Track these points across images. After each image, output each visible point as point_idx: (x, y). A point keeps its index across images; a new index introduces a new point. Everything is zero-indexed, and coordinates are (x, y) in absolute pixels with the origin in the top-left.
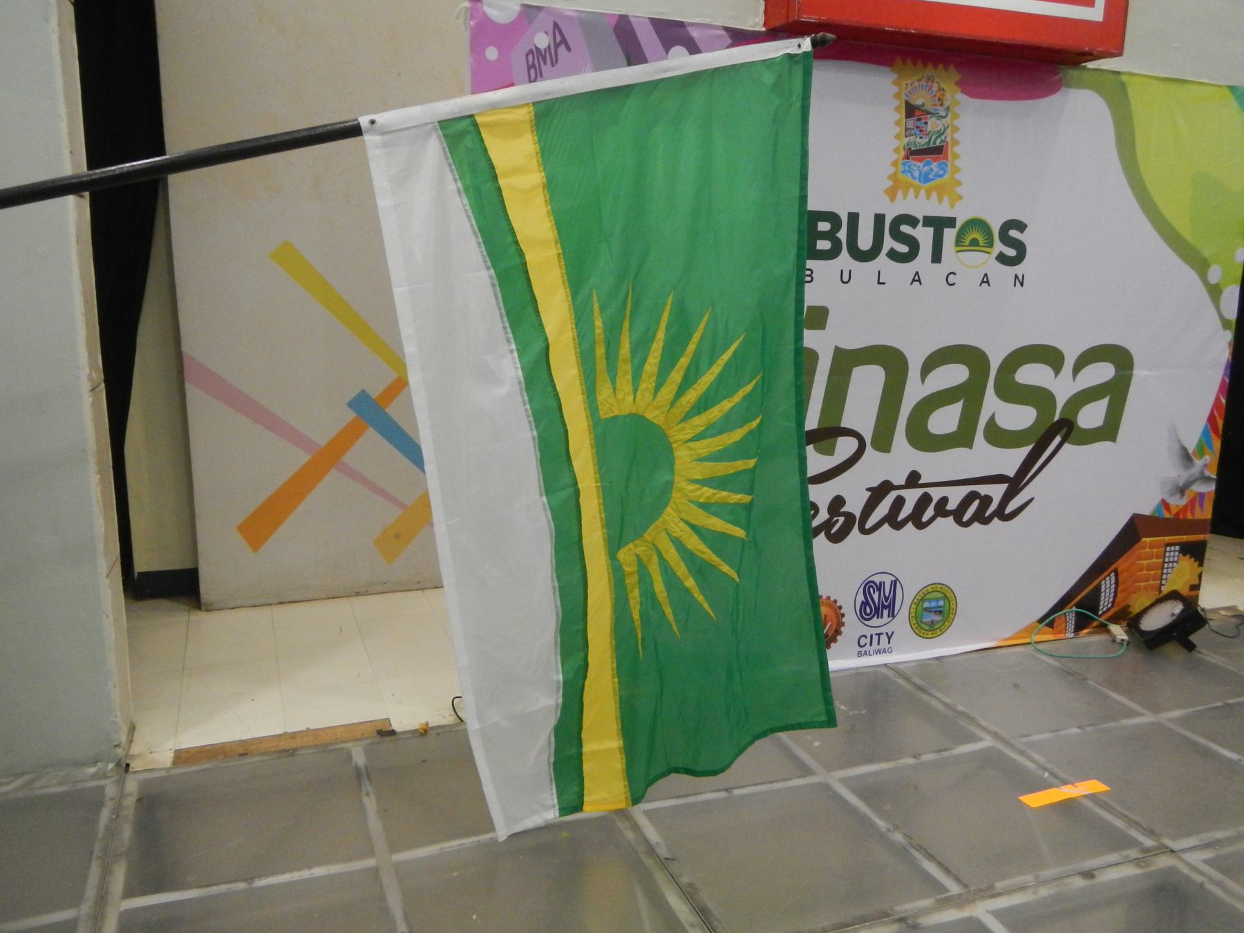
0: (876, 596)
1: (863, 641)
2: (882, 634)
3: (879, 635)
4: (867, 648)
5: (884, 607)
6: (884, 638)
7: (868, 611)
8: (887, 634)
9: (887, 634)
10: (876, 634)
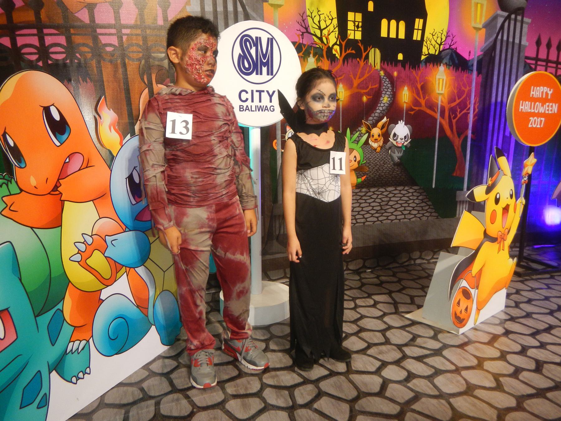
0: (253, 51)
1: (244, 96)
2: (263, 91)
3: (260, 92)
4: (249, 103)
6: (265, 96)
7: (247, 65)
8: (268, 92)
9: (268, 92)
10: (257, 91)
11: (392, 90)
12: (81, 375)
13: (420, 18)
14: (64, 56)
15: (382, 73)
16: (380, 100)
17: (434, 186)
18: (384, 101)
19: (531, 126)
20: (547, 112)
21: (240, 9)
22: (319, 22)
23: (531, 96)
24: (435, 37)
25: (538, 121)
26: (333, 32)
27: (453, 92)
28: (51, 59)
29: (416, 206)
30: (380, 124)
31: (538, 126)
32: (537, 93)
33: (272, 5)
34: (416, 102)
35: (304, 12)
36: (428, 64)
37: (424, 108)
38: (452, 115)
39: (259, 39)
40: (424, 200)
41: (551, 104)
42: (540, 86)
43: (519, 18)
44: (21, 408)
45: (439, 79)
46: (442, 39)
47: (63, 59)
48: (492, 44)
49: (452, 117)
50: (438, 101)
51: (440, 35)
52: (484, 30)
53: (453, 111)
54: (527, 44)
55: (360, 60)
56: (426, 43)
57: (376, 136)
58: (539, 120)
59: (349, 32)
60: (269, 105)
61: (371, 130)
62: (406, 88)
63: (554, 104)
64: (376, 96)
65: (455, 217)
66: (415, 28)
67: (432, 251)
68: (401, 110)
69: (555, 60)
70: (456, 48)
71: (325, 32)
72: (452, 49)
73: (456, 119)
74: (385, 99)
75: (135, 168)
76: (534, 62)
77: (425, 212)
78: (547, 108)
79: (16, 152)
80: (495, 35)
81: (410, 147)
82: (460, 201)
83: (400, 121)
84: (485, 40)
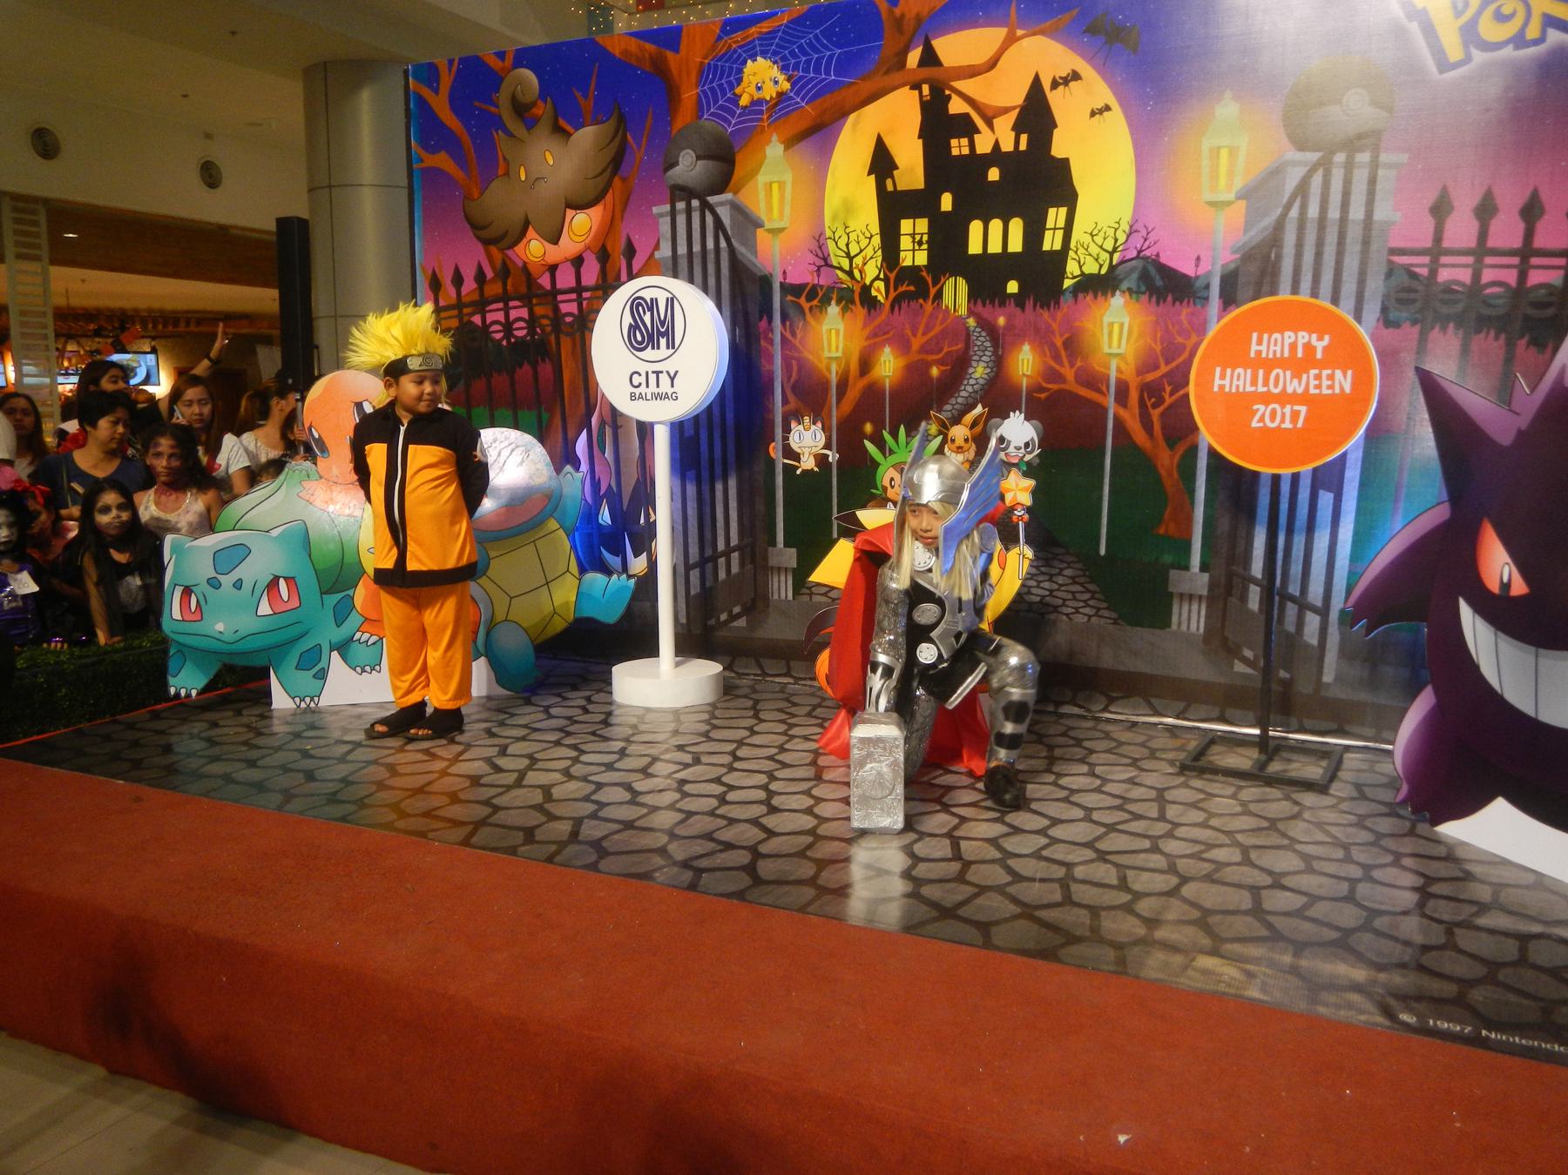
0: (647, 318)
1: (636, 379)
2: (662, 372)
3: (657, 373)
4: (643, 389)
5: (661, 334)
6: (664, 378)
7: (639, 338)
8: (668, 372)
9: (668, 372)
10: (653, 372)
11: (995, 353)
12: (368, 669)
13: (1058, 206)
14: (525, 331)
15: (971, 322)
16: (967, 373)
17: (1103, 552)
18: (977, 375)
19: (1261, 425)
20: (1313, 391)
21: (723, 244)
22: (847, 245)
23: (1252, 355)
24: (1099, 239)
25: (1283, 415)
26: (872, 258)
27: (1152, 349)
28: (516, 337)
29: (1058, 590)
30: (969, 418)
31: (1287, 425)
32: (1272, 348)
33: (770, 231)
34: (1052, 375)
35: (822, 234)
36: (1081, 296)
37: (1072, 385)
38: (1150, 400)
39: (654, 301)
40: (1077, 580)
41: (1326, 372)
42: (1282, 332)
43: (1364, 157)
44: (296, 668)
45: (1111, 325)
46: (1116, 240)
47: (522, 337)
48: (1268, 232)
49: (1149, 404)
50: (1109, 368)
51: (1111, 232)
52: (1242, 204)
53: (1151, 391)
55: (925, 300)
56: (1076, 252)
57: (960, 442)
58: (1288, 409)
59: (902, 254)
61: (948, 430)
62: (1026, 347)
63: (1338, 373)
64: (959, 367)
65: (1168, 630)
66: (1048, 227)
67: (1103, 693)
68: (1018, 391)
69: (1517, 242)
70: (1158, 255)
71: (858, 261)
72: (1147, 258)
73: (1162, 408)
74: (979, 371)
76: (1426, 260)
77: (1081, 604)
78: (1313, 383)
79: (320, 442)
80: (1280, 209)
81: (1039, 464)
82: (1181, 596)
83: (1014, 412)
84: (1246, 225)
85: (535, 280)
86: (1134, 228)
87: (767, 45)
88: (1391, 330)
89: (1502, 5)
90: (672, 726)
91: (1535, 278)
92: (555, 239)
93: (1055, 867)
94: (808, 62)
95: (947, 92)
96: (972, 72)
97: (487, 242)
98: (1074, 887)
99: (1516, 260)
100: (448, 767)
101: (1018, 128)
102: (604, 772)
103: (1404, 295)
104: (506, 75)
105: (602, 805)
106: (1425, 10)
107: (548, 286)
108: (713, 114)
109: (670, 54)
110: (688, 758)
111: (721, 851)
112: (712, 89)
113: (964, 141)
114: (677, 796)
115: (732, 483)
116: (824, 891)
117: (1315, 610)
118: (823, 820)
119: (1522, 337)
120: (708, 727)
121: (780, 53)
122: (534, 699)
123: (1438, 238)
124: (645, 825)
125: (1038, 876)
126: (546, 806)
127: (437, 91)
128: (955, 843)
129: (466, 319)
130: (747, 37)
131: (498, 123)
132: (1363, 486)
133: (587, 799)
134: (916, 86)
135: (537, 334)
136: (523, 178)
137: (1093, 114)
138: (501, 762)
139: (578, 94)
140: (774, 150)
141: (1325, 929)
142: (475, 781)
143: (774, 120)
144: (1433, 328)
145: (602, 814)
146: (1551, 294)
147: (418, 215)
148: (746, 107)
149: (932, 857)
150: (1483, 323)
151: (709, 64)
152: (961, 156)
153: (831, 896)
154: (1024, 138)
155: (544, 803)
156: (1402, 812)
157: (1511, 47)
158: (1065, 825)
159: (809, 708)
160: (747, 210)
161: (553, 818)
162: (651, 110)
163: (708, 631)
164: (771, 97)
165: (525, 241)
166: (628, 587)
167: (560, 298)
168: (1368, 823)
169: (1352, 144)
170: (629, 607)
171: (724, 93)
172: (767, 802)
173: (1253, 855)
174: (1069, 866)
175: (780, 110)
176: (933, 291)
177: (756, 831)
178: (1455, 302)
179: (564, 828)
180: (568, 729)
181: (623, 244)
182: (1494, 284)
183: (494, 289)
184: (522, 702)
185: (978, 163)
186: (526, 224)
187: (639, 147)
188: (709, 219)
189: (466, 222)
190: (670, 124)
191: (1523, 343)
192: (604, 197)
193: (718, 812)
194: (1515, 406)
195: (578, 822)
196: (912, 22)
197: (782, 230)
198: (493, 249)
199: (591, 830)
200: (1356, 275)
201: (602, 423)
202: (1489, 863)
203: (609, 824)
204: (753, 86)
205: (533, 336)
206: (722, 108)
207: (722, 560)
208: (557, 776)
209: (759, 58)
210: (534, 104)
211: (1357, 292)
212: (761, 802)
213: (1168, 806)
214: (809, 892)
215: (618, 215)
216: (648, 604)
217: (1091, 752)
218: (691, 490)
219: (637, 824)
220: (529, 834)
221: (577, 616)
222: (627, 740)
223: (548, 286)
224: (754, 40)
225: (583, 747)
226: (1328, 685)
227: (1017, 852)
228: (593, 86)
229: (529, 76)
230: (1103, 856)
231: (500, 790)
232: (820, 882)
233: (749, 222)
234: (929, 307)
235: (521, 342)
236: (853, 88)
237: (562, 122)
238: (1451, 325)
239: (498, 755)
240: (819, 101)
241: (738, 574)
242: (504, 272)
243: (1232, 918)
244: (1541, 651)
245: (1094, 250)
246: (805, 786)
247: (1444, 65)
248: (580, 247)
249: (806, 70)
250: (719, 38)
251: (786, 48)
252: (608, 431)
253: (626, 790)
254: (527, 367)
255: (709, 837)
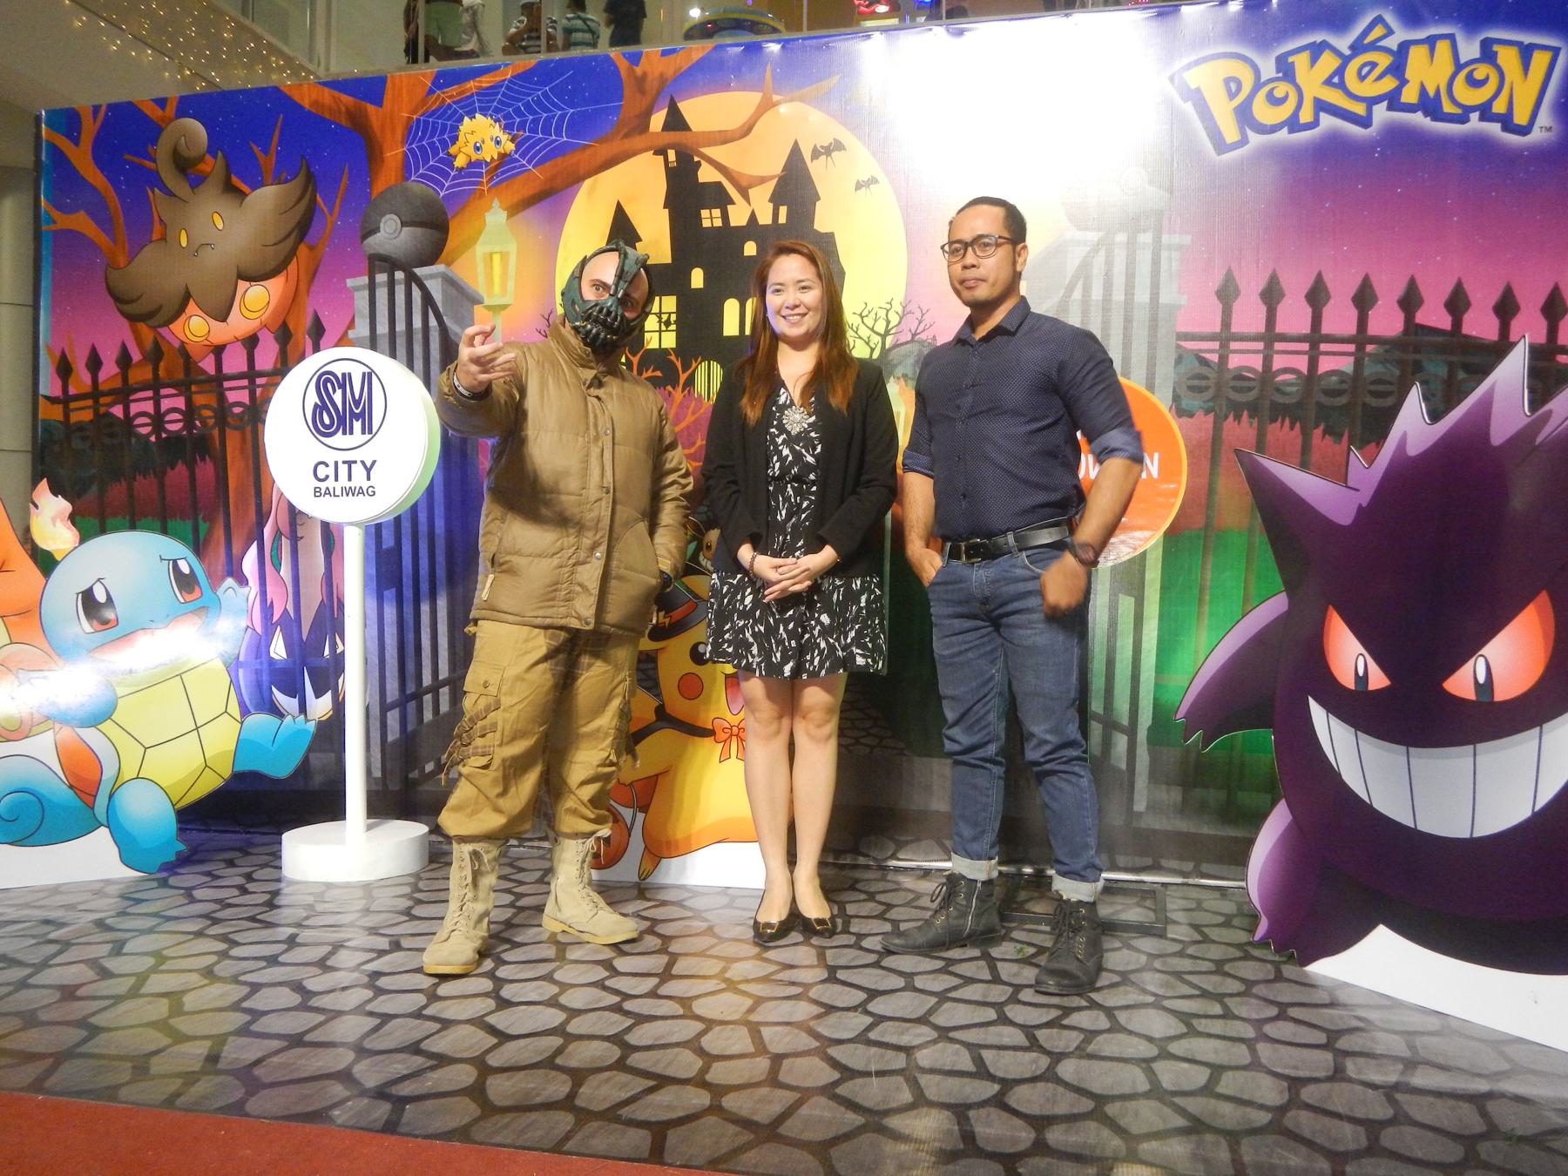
0: (338, 397)
1: (322, 471)
2: (355, 462)
3: (350, 463)
4: (330, 483)
5: (357, 417)
6: (358, 470)
7: (327, 421)
8: (363, 462)
9: (363, 462)
10: (344, 462)
14: (181, 425)
21: (433, 322)
24: (869, 321)
33: (489, 308)
39: (347, 377)
46: (888, 322)
51: (882, 313)
54: (1184, 300)
59: (647, 336)
60: (365, 485)
61: (703, 535)
72: (922, 342)
75: (99, 580)
76: (1216, 345)
77: (863, 733)
80: (1062, 291)
85: (196, 363)
86: (908, 309)
87: (488, 102)
88: (1185, 420)
89: (1273, 89)
90: (360, 904)
91: (1325, 365)
92: (224, 319)
93: (890, 1053)
94: (536, 122)
95: (696, 159)
96: (724, 138)
97: (133, 319)
98: (924, 1080)
99: (1305, 346)
100: (31, 976)
101: (777, 199)
102: (264, 968)
103: (1196, 382)
104: (167, 125)
105: (257, 1014)
106: (1198, 90)
107: (211, 370)
108: (422, 176)
109: (371, 108)
110: (383, 943)
111: (432, 1068)
112: (422, 148)
113: (717, 212)
114: (369, 994)
115: (442, 603)
116: (584, 1116)
117: (1122, 730)
118: (574, 1013)
119: (1317, 427)
120: (410, 903)
121: (502, 110)
122: (173, 881)
123: (1226, 324)
124: (321, 1039)
125: (873, 1068)
126: (172, 1021)
127: (76, 141)
128: (754, 1030)
129: (102, 410)
130: (463, 92)
131: (155, 180)
132: (1165, 589)
133: (236, 1007)
134: (661, 151)
135: (195, 427)
136: (184, 243)
137: (859, 186)
138: (112, 964)
139: (256, 149)
140: (495, 217)
141: (1248, 1110)
142: (69, 993)
143: (495, 185)
144: (1226, 417)
145: (260, 1026)
146: (1342, 382)
147: (46, 284)
148: (460, 170)
149: (728, 1052)
150: (1279, 412)
151: (418, 120)
152: (713, 227)
153: (595, 1124)
154: (783, 210)
155: (170, 1017)
156: (1256, 953)
157: (1285, 130)
158: (887, 997)
159: (538, 874)
160: (460, 282)
161: (181, 1038)
162: (346, 171)
163: (409, 785)
164: (492, 159)
165: (183, 317)
166: (305, 731)
167: (226, 384)
168: (1227, 968)
169: (1134, 223)
170: (305, 762)
171: (436, 153)
172: (495, 994)
173: (1122, 1017)
174: (907, 1050)
175: (503, 173)
176: (683, 377)
177: (482, 1034)
178: (1250, 389)
179: (199, 1052)
180: (219, 915)
181: (308, 321)
182: (1285, 370)
183: (141, 374)
184: (155, 884)
185: (730, 237)
186: (187, 297)
187: (331, 215)
188: (416, 293)
189: (106, 293)
190: (370, 188)
191: (1318, 432)
192: (286, 268)
193: (426, 1012)
194: (1350, 484)
195: (221, 1040)
196: (655, 83)
197: (504, 307)
198: (142, 327)
199: (241, 1052)
200: (1144, 366)
201: (278, 534)
202: (1380, 1007)
203: (266, 1042)
204: (471, 145)
205: (190, 433)
206: (432, 169)
207: (428, 698)
208: (195, 978)
209: (477, 115)
210: (201, 159)
211: (1147, 379)
212: (486, 995)
213: (1000, 965)
214: (565, 1120)
215: (303, 287)
216: (333, 755)
217: (889, 906)
218: (390, 612)
219: (307, 1038)
220: (141, 1065)
221: (236, 769)
222: (299, 925)
223: (211, 370)
224: (472, 95)
225: (237, 937)
226: (1140, 814)
227: (836, 1036)
228: (276, 139)
229: (196, 129)
230: (944, 1033)
231: (108, 1002)
232: (579, 1102)
233: (465, 298)
234: (678, 395)
235: (175, 439)
236: (588, 152)
237: (235, 180)
238: (1245, 413)
239: (110, 955)
240: (548, 164)
241: (447, 714)
242: (155, 355)
243: (1133, 1104)
244: (1411, 749)
245: (864, 332)
246: (543, 969)
247: (1221, 146)
248: (256, 324)
249: (534, 130)
250: (431, 92)
251: (509, 105)
252: (286, 544)
253: (293, 990)
254: (181, 467)
255: (415, 1049)
